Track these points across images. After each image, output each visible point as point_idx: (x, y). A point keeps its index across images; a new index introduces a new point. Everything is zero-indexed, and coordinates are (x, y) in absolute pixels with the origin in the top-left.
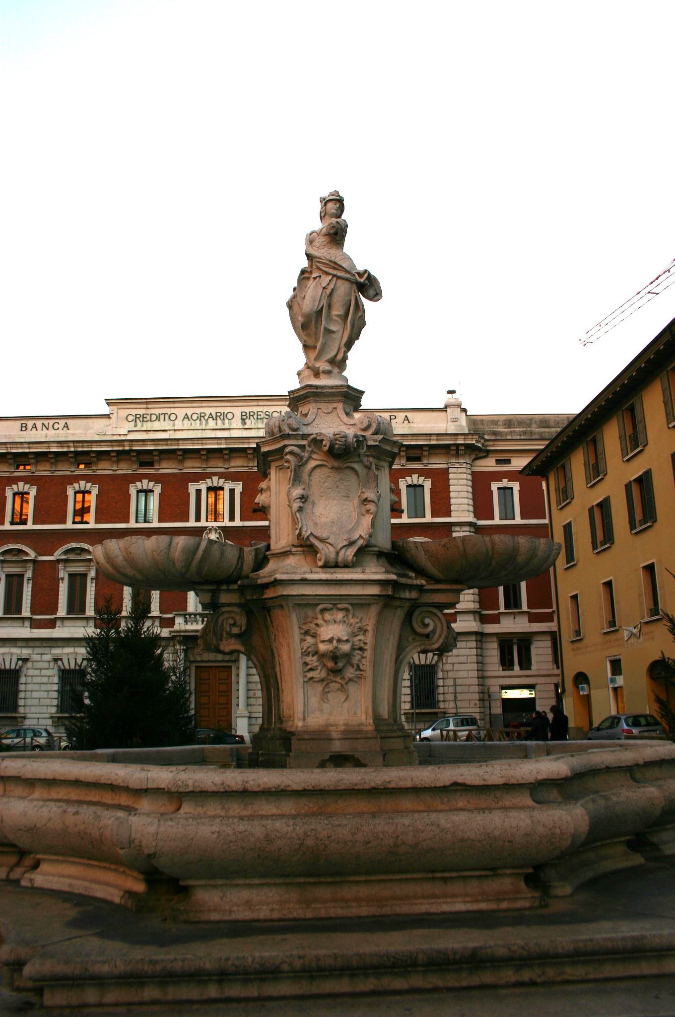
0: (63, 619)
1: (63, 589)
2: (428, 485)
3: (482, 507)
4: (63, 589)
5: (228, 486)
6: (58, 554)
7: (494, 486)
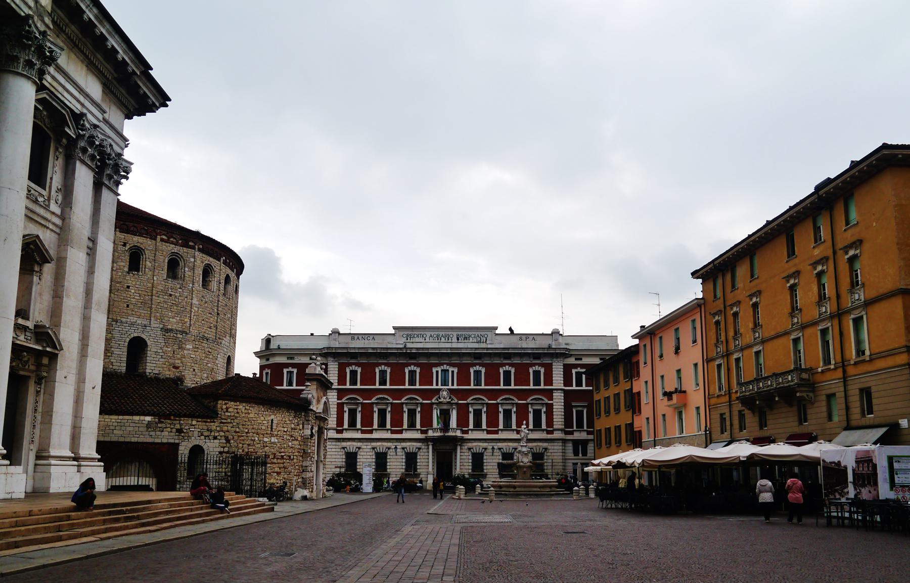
0: (346, 430)
1: (376, 416)
2: (542, 370)
3: (567, 381)
4: (376, 416)
5: (451, 369)
6: (373, 400)
7: (574, 371)
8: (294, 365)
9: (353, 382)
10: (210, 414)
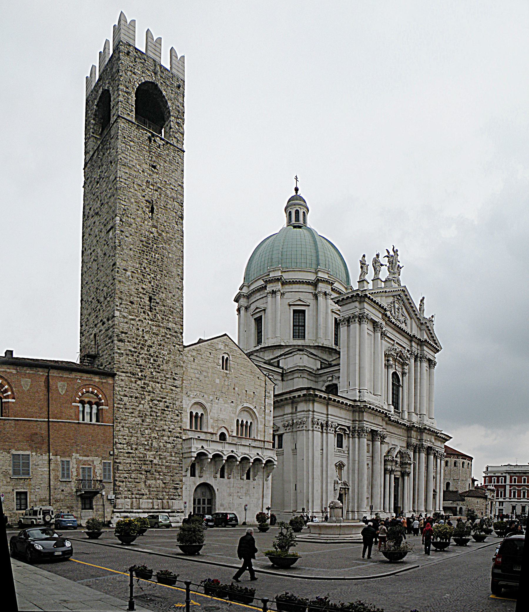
8: (503, 476)
9: (515, 482)
10: (463, 500)
